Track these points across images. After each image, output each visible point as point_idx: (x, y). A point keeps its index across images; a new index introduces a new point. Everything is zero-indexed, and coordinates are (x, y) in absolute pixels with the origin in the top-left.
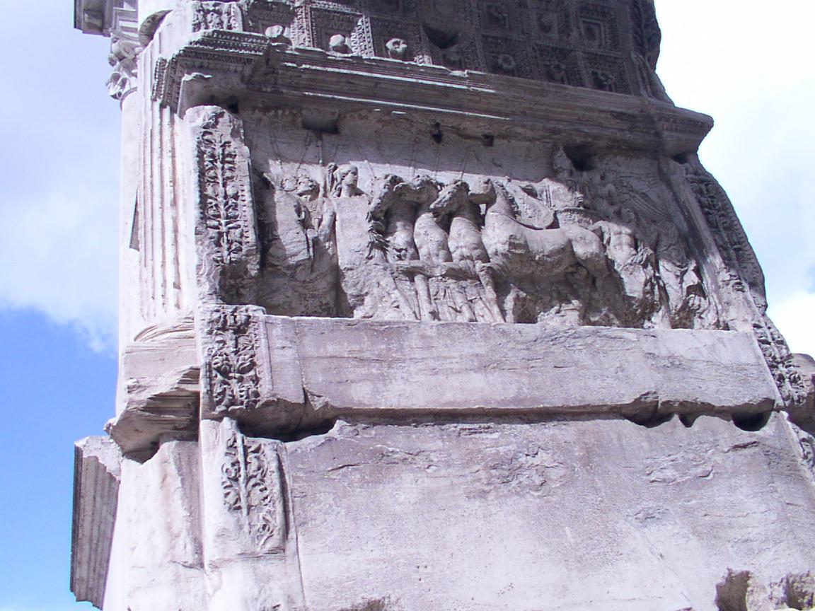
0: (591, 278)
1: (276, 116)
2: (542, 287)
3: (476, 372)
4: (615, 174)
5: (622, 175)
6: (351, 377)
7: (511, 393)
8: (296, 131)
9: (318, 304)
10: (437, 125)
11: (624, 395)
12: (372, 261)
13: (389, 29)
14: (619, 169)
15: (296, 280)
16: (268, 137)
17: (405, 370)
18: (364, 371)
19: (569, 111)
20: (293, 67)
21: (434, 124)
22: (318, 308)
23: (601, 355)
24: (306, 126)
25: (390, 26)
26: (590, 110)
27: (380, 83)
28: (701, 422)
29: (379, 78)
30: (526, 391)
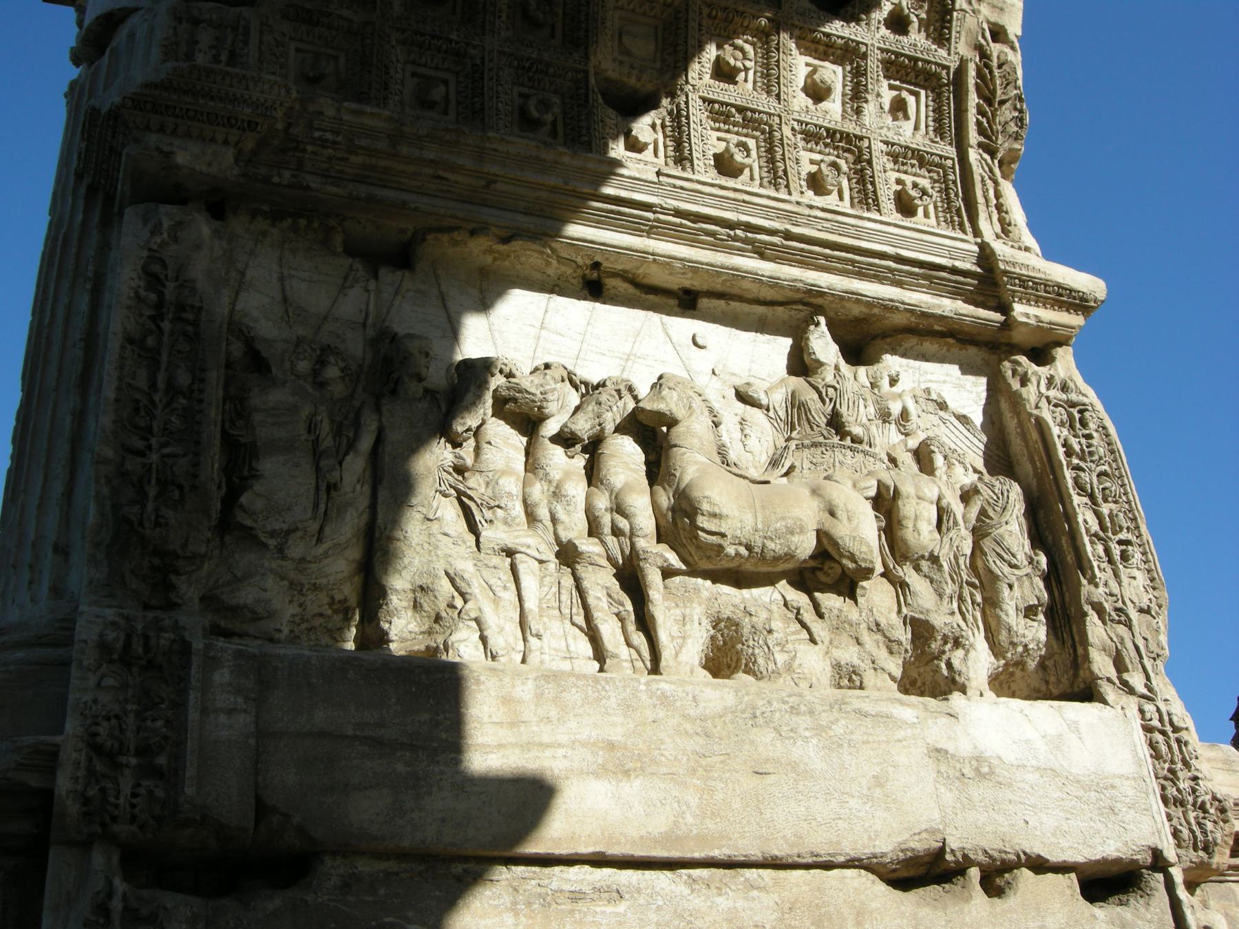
0: (848, 581)
3: (596, 775)
4: (917, 375)
5: (929, 377)
7: (659, 824)
9: (326, 600)
10: (596, 265)
12: (435, 527)
13: (531, 74)
15: (284, 558)
20: (335, 143)
21: (589, 262)
22: (327, 607)
24: (351, 250)
25: (534, 69)
27: (495, 182)
29: (496, 175)
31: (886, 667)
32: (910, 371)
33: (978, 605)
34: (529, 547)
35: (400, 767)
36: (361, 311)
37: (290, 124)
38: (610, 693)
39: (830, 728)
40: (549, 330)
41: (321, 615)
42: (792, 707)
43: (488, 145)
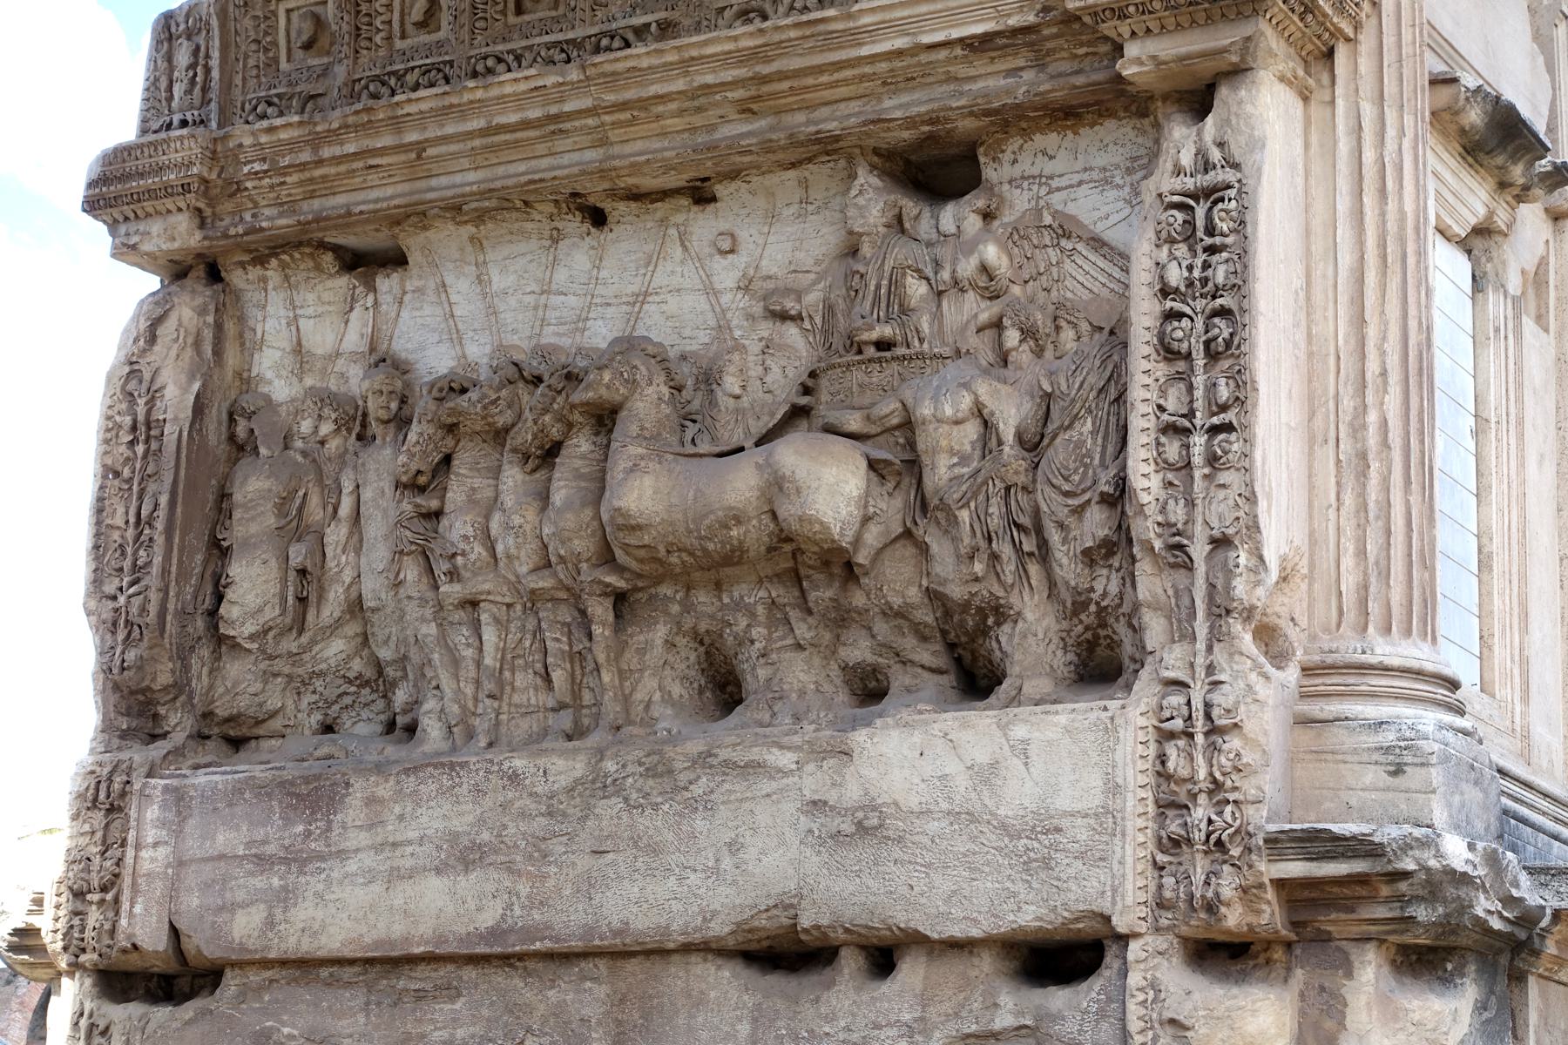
1: (284, 266)
2: (736, 594)
4: (1035, 187)
5: (1055, 183)
6: (241, 896)
8: (330, 283)
11: (715, 913)
14: (1049, 167)
15: (271, 658)
16: (282, 312)
17: (323, 876)
18: (258, 882)
19: (848, 73)
20: (266, 172)
23: (699, 815)
26: (899, 53)
27: (424, 150)
28: (911, 972)
30: (518, 912)
31: (916, 657)
32: (1025, 184)
33: (1031, 554)
34: (489, 593)
35: (276, 882)
36: (362, 335)
37: (222, 167)
38: (464, 779)
39: (686, 789)
40: (548, 292)
41: (347, 694)
42: (647, 769)
43: (400, 112)
